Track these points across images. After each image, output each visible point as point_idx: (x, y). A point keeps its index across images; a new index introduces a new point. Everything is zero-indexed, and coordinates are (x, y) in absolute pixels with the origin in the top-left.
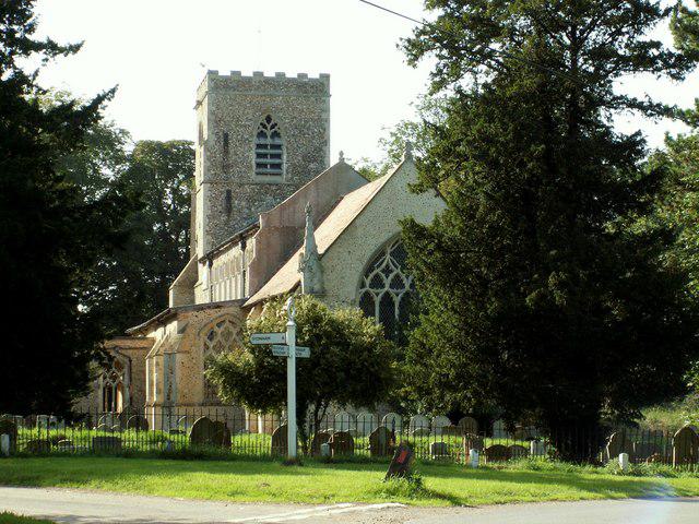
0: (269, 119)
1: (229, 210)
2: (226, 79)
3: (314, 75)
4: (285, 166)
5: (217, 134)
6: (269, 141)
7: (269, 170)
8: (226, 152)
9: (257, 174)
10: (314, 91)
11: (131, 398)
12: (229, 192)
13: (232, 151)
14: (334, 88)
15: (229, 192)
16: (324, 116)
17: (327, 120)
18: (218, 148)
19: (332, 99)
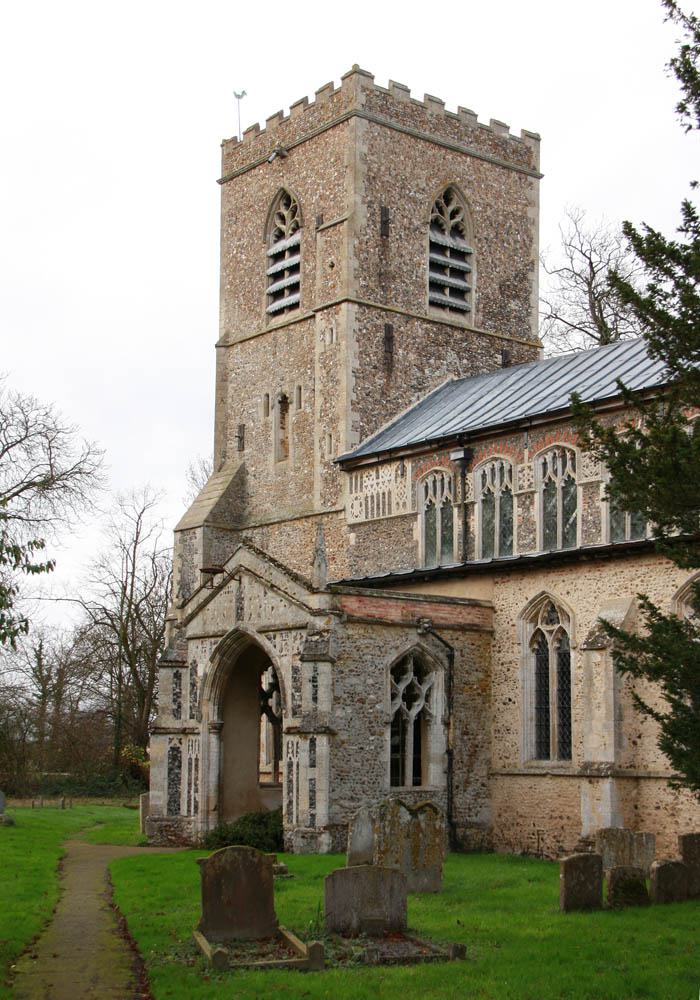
0: (447, 197)
1: (388, 364)
2: (385, 95)
4: (474, 296)
5: (370, 205)
6: (447, 240)
7: (447, 298)
8: (384, 246)
9: (433, 303)
10: (517, 157)
11: (449, 752)
12: (389, 329)
13: (393, 246)
14: (545, 165)
15: (389, 329)
17: (535, 223)
18: (372, 234)
19: (545, 187)
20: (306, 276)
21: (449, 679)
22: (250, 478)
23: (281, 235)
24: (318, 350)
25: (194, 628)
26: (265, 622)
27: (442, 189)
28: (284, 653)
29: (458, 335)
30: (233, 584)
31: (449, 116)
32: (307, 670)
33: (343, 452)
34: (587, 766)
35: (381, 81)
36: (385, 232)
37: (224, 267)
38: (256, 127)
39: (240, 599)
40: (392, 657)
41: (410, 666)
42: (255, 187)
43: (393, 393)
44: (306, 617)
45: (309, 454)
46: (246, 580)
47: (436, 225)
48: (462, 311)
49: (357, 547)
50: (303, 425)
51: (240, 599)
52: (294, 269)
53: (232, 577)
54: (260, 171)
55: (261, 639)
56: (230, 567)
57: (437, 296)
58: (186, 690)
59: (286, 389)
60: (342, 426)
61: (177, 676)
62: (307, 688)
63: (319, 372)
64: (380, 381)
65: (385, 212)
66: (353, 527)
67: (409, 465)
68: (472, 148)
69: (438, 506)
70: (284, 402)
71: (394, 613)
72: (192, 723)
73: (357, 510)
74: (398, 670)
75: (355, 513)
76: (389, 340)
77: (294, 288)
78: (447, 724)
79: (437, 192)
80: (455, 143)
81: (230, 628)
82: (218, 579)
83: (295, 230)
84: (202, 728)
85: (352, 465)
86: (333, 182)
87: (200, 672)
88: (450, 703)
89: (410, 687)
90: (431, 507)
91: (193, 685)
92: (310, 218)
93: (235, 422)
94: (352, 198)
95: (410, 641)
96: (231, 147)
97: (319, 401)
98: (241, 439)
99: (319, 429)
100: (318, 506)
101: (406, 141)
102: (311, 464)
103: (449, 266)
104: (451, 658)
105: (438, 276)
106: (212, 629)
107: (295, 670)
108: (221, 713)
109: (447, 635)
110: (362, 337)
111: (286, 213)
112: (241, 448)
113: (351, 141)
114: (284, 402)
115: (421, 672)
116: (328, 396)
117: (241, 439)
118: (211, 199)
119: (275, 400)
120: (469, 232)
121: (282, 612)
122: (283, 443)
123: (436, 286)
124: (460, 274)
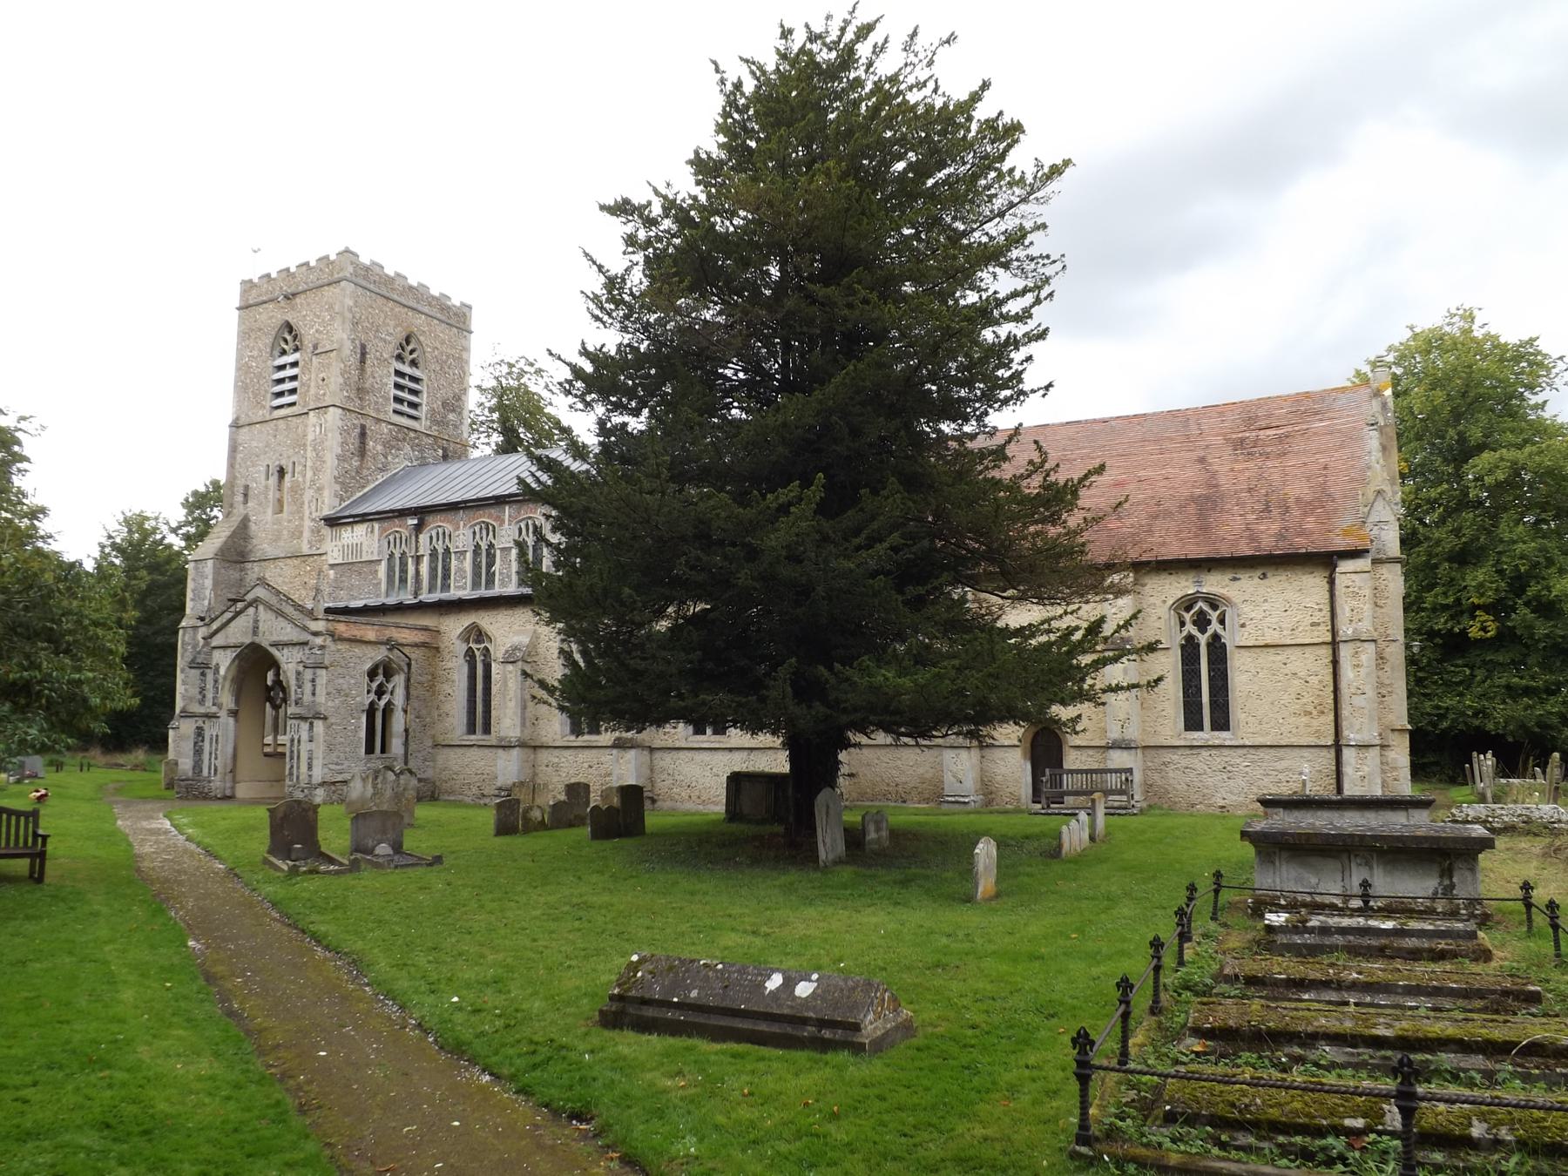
1: (362, 451)
2: (367, 269)
3: (456, 301)
4: (424, 408)
5: (353, 341)
6: (406, 369)
7: (405, 408)
8: (362, 370)
9: (395, 412)
11: (406, 731)
12: (363, 427)
13: (369, 370)
14: (475, 324)
15: (363, 427)
16: (465, 356)
18: (354, 360)
20: (303, 384)
21: (408, 680)
22: (253, 527)
23: (284, 352)
24: (310, 437)
25: (215, 642)
26: (275, 638)
27: (404, 334)
28: (289, 661)
29: (412, 434)
30: (251, 610)
31: (411, 287)
32: (308, 674)
33: (326, 512)
34: (502, 739)
35: (365, 259)
36: (363, 361)
37: (238, 369)
38: (268, 275)
39: (256, 621)
40: (368, 666)
41: (381, 671)
42: (264, 317)
43: (365, 472)
44: (305, 637)
45: (300, 511)
46: (261, 608)
47: (399, 358)
48: (415, 418)
49: (336, 580)
50: (296, 490)
51: (256, 621)
52: (294, 378)
53: (250, 605)
54: (271, 306)
55: (273, 651)
56: (249, 597)
57: (399, 407)
58: (210, 685)
59: (283, 463)
60: (326, 493)
61: (203, 674)
62: (308, 687)
63: (310, 453)
64: (356, 464)
65: (363, 347)
66: (332, 566)
67: (376, 526)
68: (426, 309)
69: (397, 555)
70: (282, 472)
71: (371, 635)
72: (214, 709)
73: (335, 554)
74: (372, 674)
75: (335, 556)
76: (363, 434)
77: (293, 391)
78: (405, 711)
79: (400, 334)
80: (415, 305)
81: (248, 641)
82: (240, 605)
83: (296, 350)
84: (223, 714)
85: (333, 522)
86: (326, 324)
87: (222, 671)
88: (408, 696)
89: (381, 686)
90: (392, 555)
91: (216, 681)
92: (308, 343)
93: (241, 482)
94: (341, 336)
95: (380, 654)
96: (248, 286)
97: (309, 474)
98: (246, 495)
99: (309, 494)
100: (306, 550)
101: (380, 301)
102: (302, 519)
103: (407, 388)
104: (409, 665)
105: (400, 393)
106: (232, 641)
107: (298, 673)
108: (237, 702)
109: (406, 650)
110: (345, 432)
111: (289, 338)
112: (246, 502)
113: (344, 296)
114: (282, 472)
115: (388, 675)
116: (316, 471)
117: (246, 495)
118: (230, 322)
119: (274, 470)
120: (421, 365)
121: (289, 633)
122: (280, 502)
123: (398, 400)
124: (415, 392)
